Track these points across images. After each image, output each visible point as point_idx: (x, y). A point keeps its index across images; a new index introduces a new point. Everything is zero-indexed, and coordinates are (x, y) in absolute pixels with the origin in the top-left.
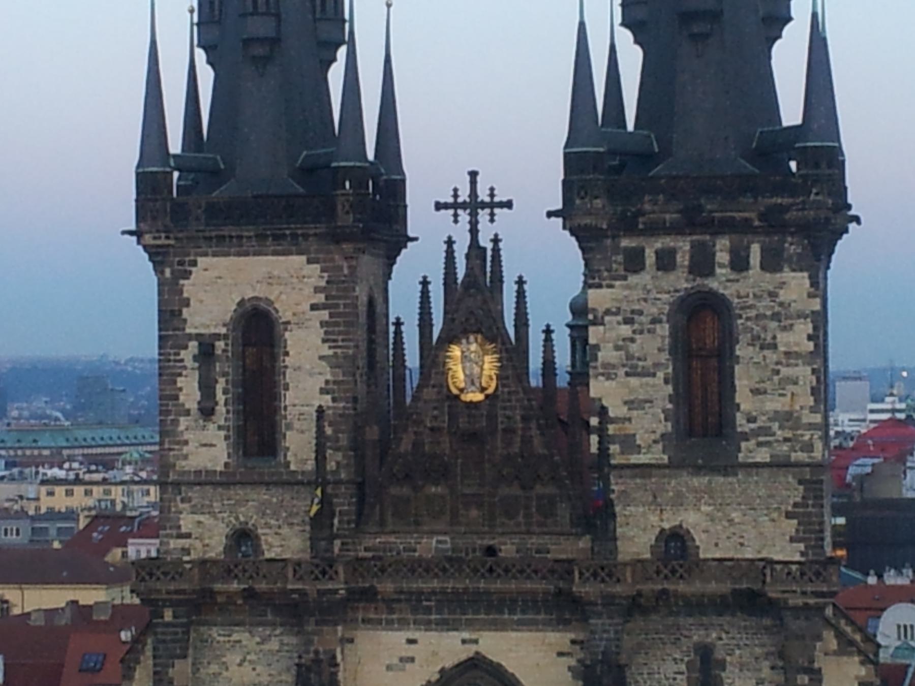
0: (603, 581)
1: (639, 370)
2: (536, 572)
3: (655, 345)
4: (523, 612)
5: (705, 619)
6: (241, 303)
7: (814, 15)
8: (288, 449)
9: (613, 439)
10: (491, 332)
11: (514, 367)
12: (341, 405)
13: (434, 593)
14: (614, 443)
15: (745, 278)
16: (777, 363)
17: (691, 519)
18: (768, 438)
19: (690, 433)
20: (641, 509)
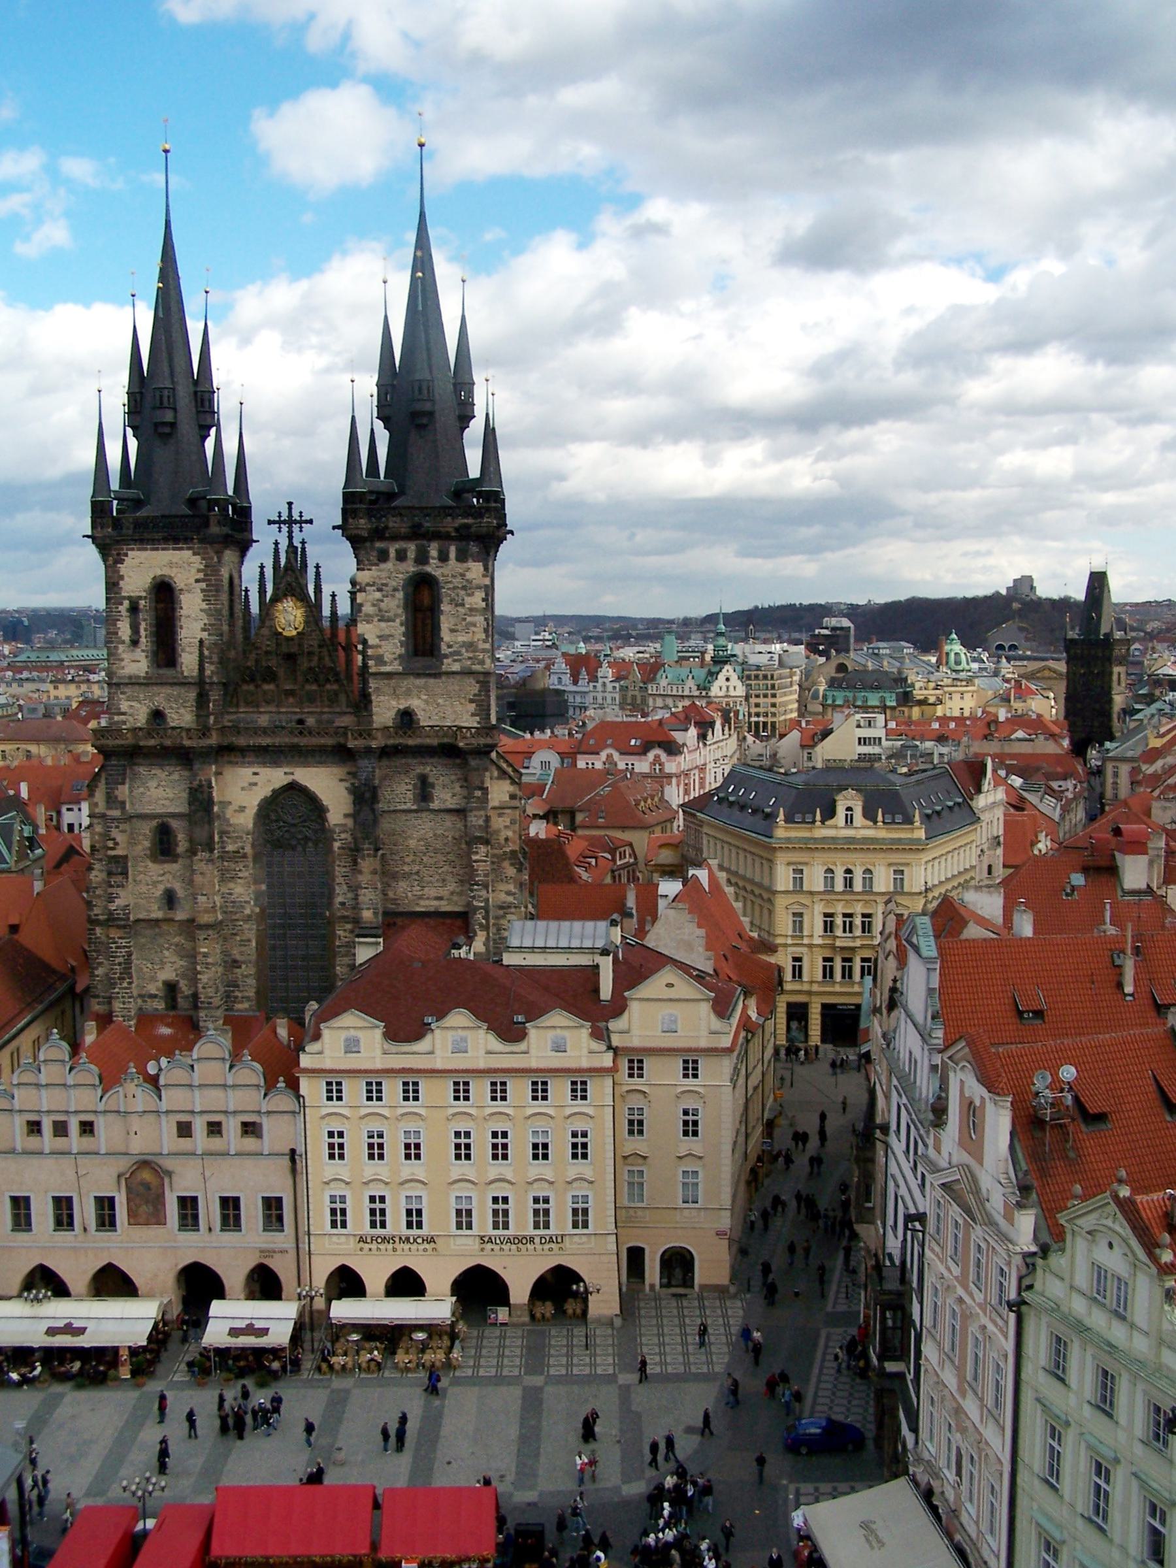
3: (395, 604)
5: (424, 761)
7: (487, 415)
10: (300, 595)
17: (416, 703)
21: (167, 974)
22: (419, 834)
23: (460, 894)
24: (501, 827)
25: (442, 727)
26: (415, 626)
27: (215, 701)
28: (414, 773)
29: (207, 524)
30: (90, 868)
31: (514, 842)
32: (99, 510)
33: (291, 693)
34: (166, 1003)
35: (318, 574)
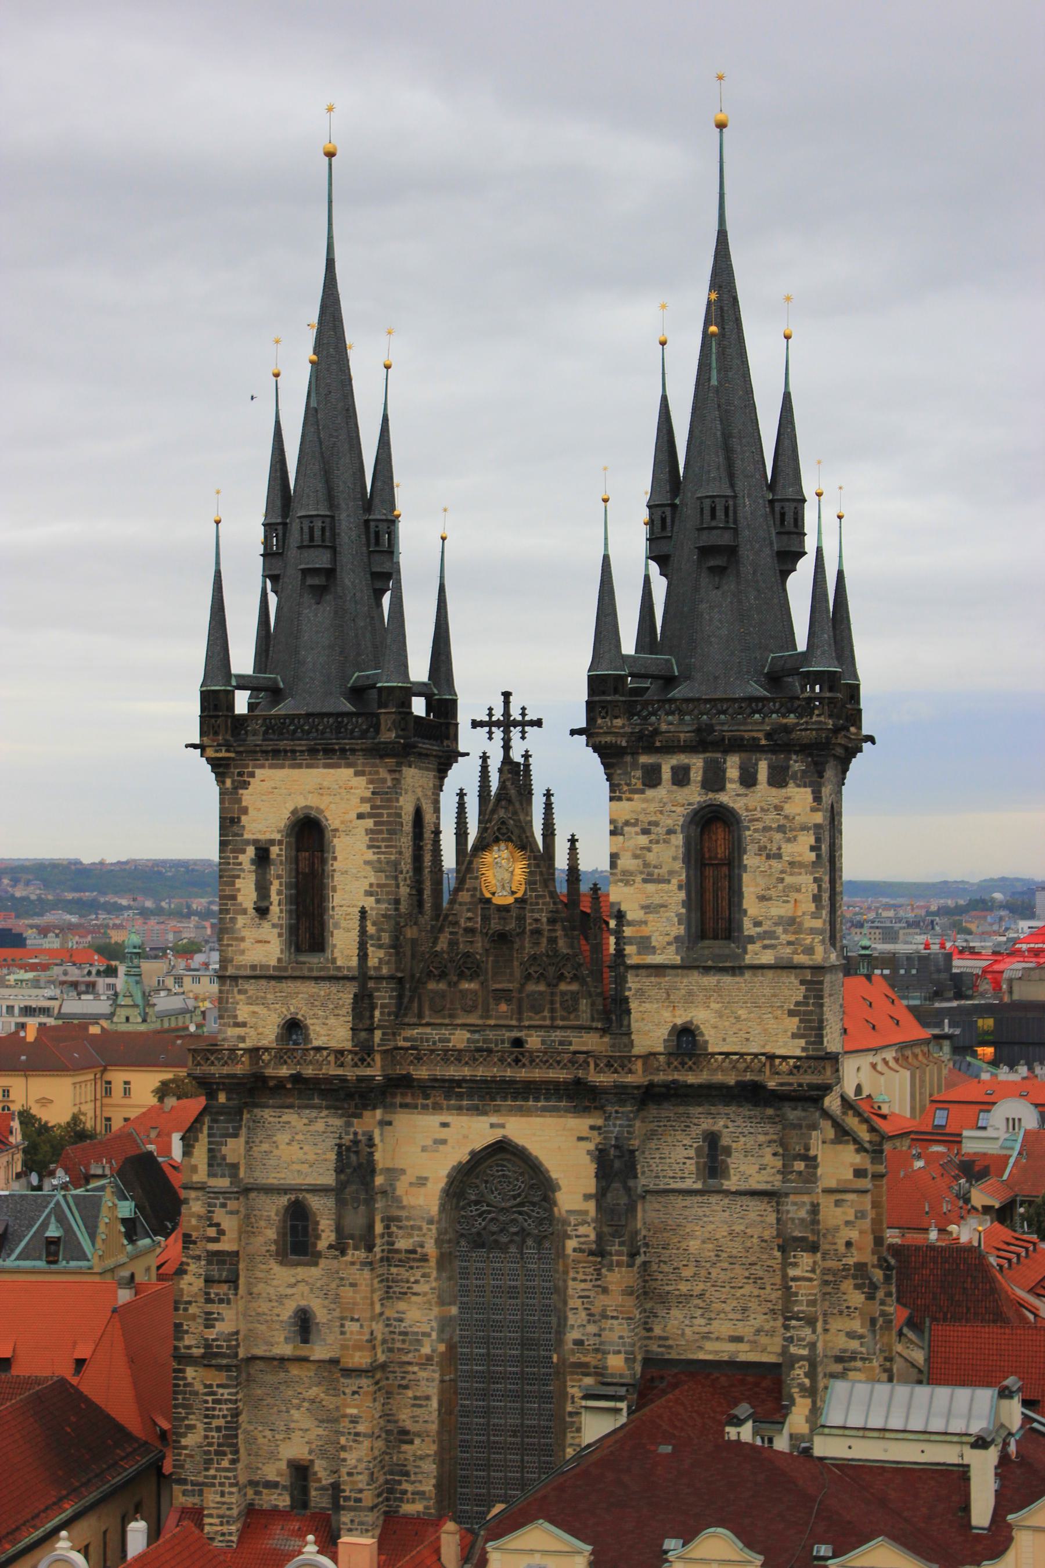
0: (616, 1072)
1: (655, 877)
2: (559, 1062)
3: (670, 854)
4: (547, 1099)
5: (713, 1109)
6: (294, 812)
7: (819, 551)
8: (334, 946)
9: (630, 941)
11: (541, 873)
12: (384, 906)
13: (464, 1080)
14: (631, 944)
15: (754, 792)
16: (782, 872)
18: (773, 942)
19: (703, 936)
20: (656, 1006)
21: (295, 1449)
22: (711, 1232)
23: (771, 1333)
24: (840, 1223)
25: (742, 1055)
26: (702, 891)
27: (383, 1006)
28: (696, 1131)
29: (377, 731)
30: (181, 1271)
31: (859, 1249)
32: (214, 705)
33: (503, 995)
34: (292, 1497)
35: (548, 807)
